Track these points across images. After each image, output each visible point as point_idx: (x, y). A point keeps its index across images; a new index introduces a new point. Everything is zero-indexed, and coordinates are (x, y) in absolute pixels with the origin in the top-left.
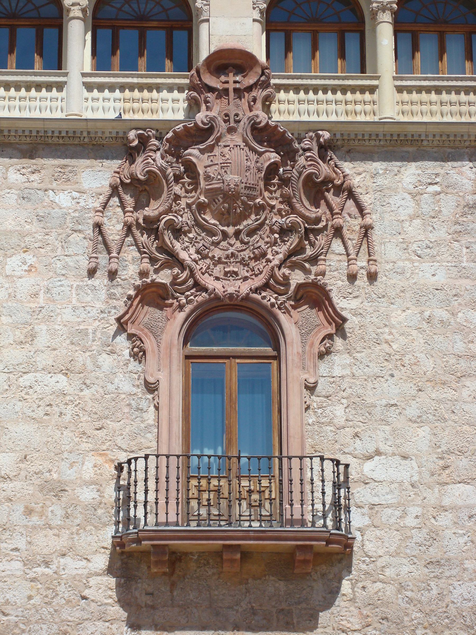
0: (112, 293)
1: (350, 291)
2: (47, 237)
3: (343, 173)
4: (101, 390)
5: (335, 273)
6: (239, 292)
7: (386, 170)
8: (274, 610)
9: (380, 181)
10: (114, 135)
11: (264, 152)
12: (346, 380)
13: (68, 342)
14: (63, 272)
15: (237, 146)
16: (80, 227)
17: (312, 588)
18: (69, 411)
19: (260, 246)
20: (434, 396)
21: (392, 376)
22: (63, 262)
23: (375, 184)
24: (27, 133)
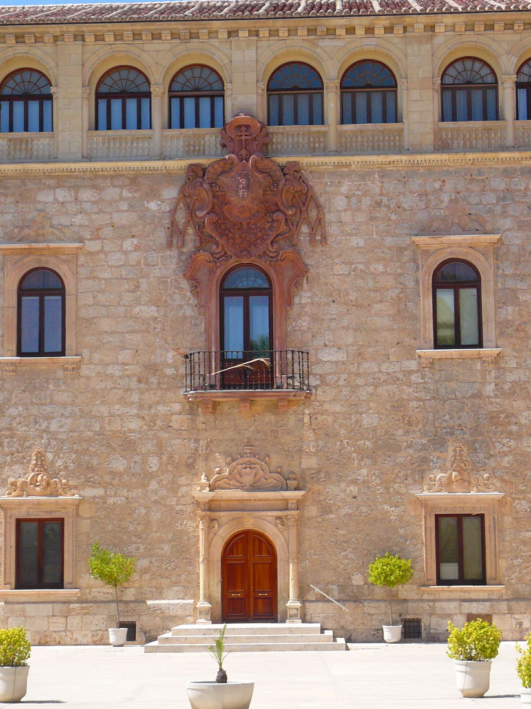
7: (332, 182)
8: (269, 430)
10: (179, 168)
17: (289, 418)
18: (159, 326)
21: (334, 301)
24: (132, 169)
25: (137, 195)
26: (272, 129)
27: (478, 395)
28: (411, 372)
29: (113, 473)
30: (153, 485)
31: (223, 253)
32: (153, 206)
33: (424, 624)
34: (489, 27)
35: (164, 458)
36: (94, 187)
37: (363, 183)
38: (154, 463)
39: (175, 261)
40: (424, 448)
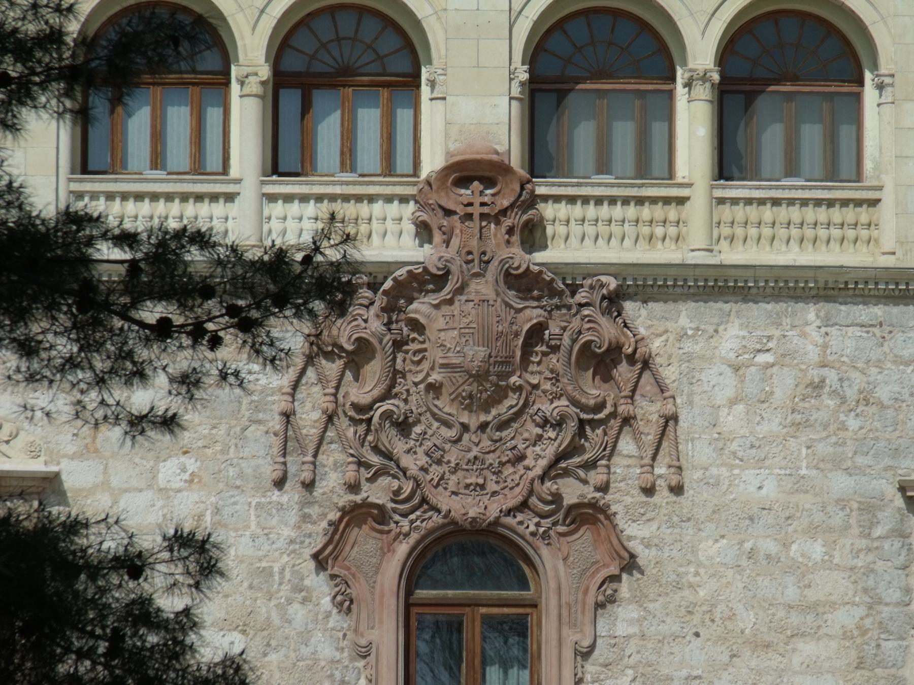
0: (305, 514)
1: (642, 511)
2: (214, 431)
3: (634, 335)
4: (292, 655)
5: (622, 484)
6: (484, 514)
7: (698, 329)
9: (688, 346)
11: (521, 310)
12: (633, 642)
13: (246, 584)
14: (238, 483)
15: (484, 301)
16: (261, 416)
19: (516, 447)
20: (753, 664)
21: (697, 635)
22: (237, 469)
23: (681, 352)
31: (416, 500)
37: (777, 333)
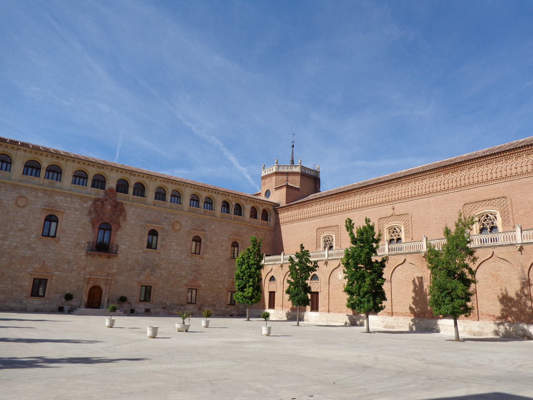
25: (82, 202)
26: (117, 193)
27: (154, 260)
28: (141, 253)
29: (64, 269)
30: (74, 273)
32: (85, 205)
33: (135, 310)
34: (168, 182)
35: (78, 266)
36: (71, 198)
38: (75, 267)
39: (89, 219)
40: (141, 270)
